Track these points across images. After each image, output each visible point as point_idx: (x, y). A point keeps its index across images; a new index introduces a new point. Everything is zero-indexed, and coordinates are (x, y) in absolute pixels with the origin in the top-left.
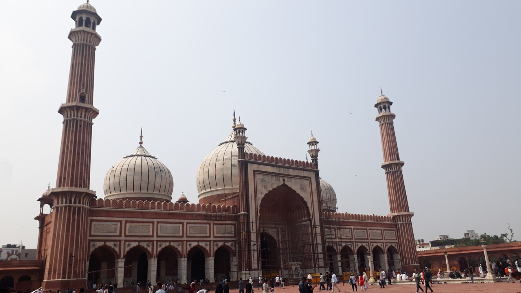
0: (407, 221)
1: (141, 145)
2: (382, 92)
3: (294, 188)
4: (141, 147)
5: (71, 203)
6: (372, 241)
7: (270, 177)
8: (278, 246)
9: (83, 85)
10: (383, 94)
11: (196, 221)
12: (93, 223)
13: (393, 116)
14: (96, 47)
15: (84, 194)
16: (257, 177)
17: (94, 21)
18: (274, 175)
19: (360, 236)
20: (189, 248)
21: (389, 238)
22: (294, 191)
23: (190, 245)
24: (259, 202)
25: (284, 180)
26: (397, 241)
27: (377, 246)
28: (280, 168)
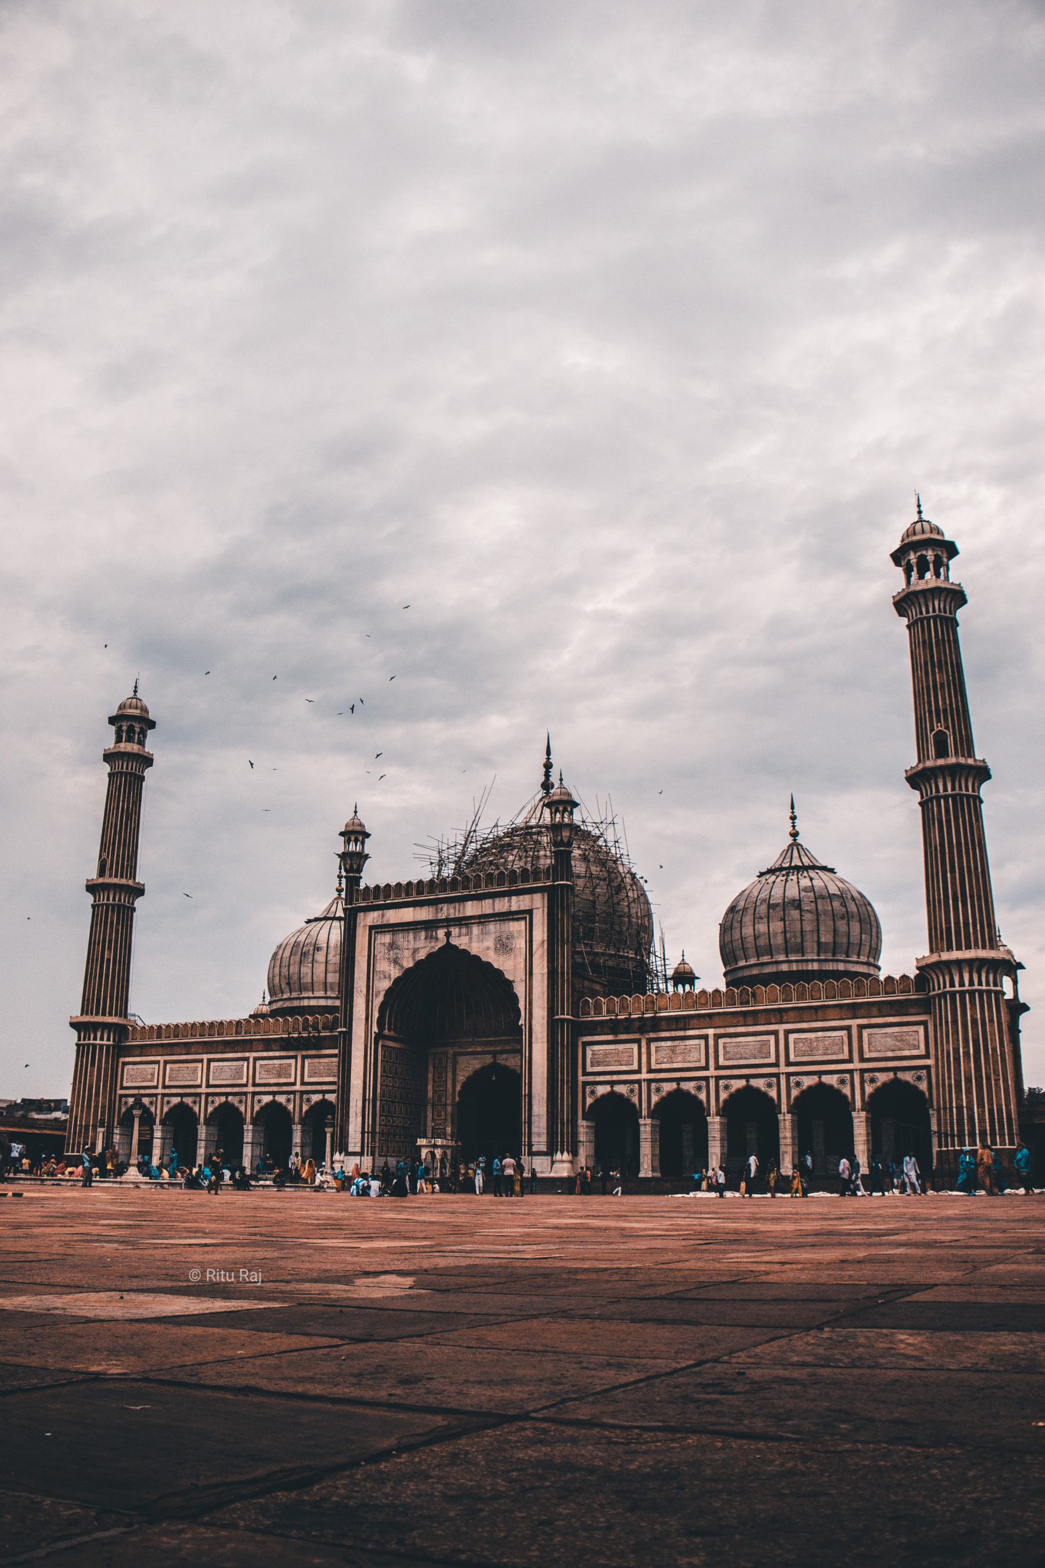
0: (948, 986)
2: (922, 508)
3: (475, 949)
7: (411, 935)
10: (924, 516)
11: (271, 1054)
12: (126, 1067)
15: (90, 1025)
16: (378, 942)
18: (419, 929)
19: (741, 1058)
20: (257, 1108)
21: (890, 1054)
22: (477, 958)
23: (259, 1101)
24: (378, 1001)
25: (448, 935)
26: (930, 1062)
27: (821, 1085)
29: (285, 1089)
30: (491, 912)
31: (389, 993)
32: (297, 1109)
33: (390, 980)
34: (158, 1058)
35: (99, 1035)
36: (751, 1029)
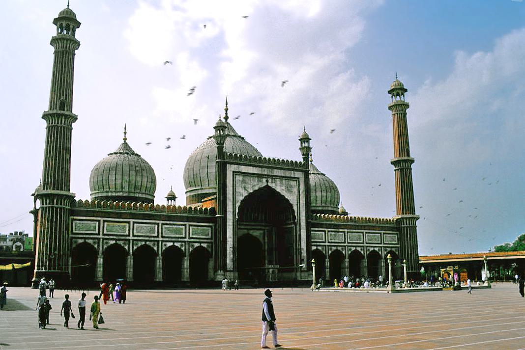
1: (125, 142)
3: (278, 189)
4: (125, 143)
5: (54, 204)
6: (367, 245)
8: (263, 249)
9: (63, 92)
11: (171, 222)
12: (74, 222)
13: (407, 106)
14: (76, 52)
17: (74, 27)
20: (164, 248)
21: (390, 242)
23: (165, 245)
24: (238, 205)
25: (267, 181)
28: (264, 169)
29: (180, 240)
30: (284, 175)
31: (242, 201)
32: (187, 251)
33: (243, 196)
34: (99, 219)
35: (65, 202)
36: (357, 231)
